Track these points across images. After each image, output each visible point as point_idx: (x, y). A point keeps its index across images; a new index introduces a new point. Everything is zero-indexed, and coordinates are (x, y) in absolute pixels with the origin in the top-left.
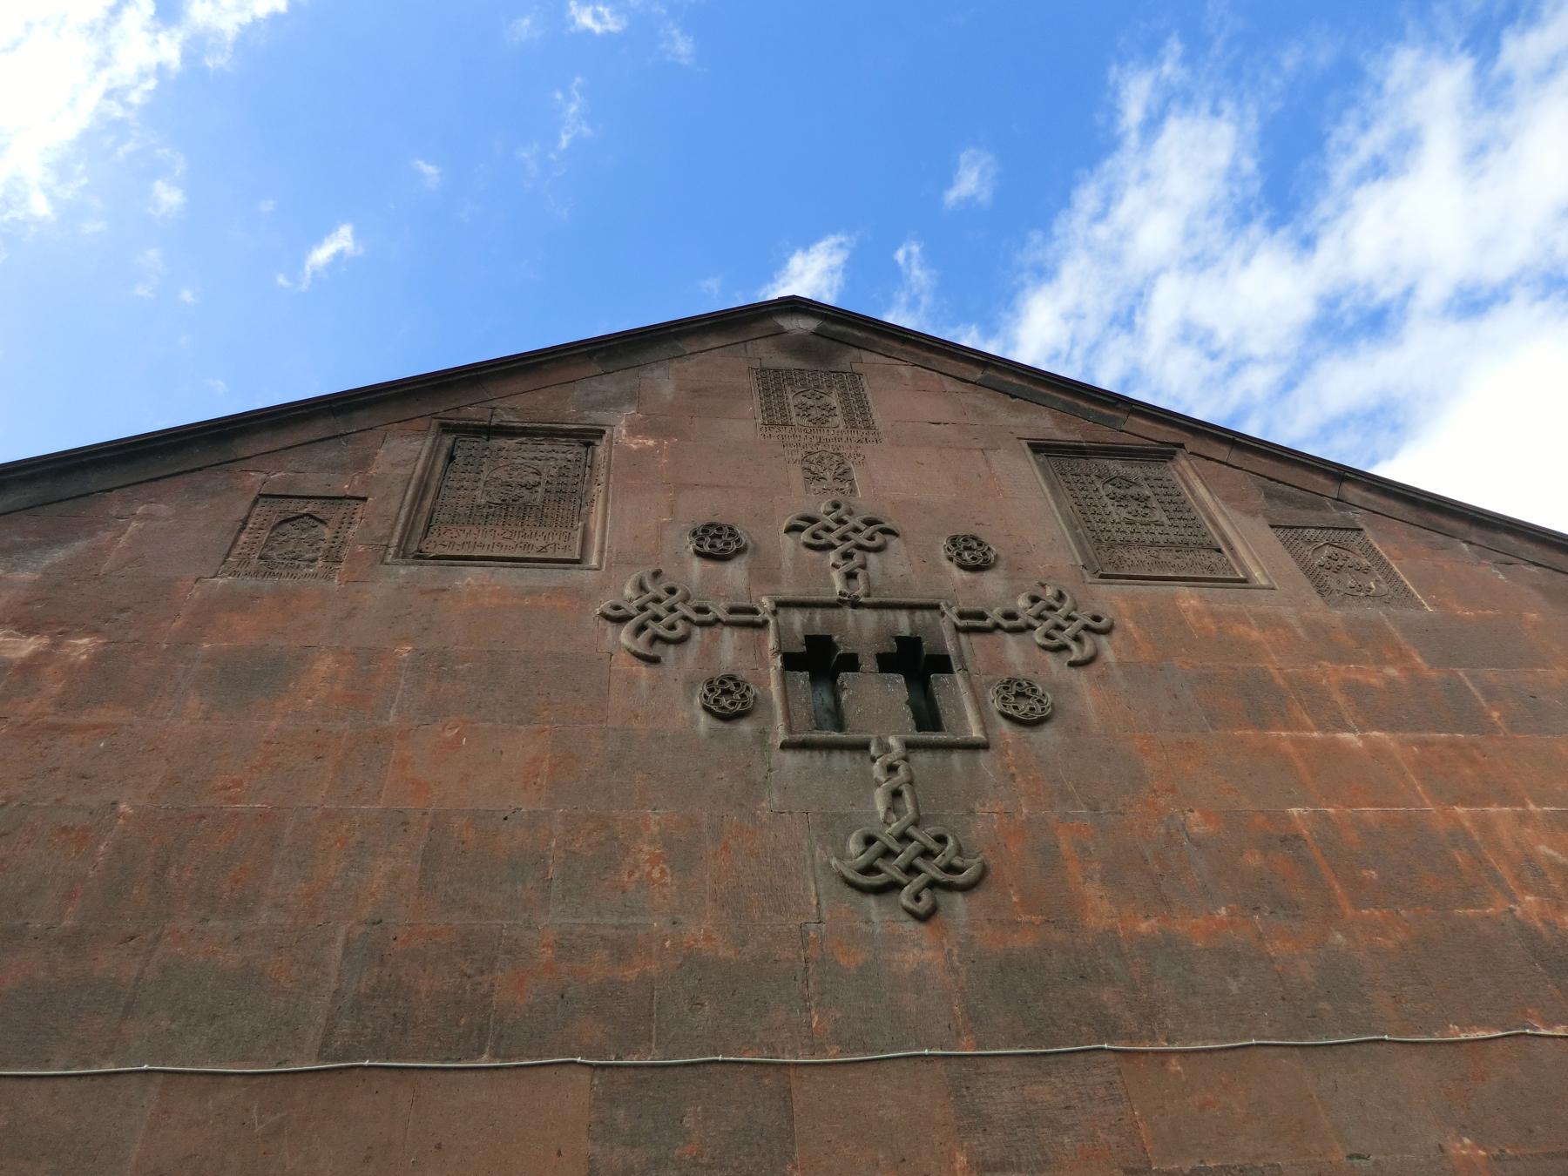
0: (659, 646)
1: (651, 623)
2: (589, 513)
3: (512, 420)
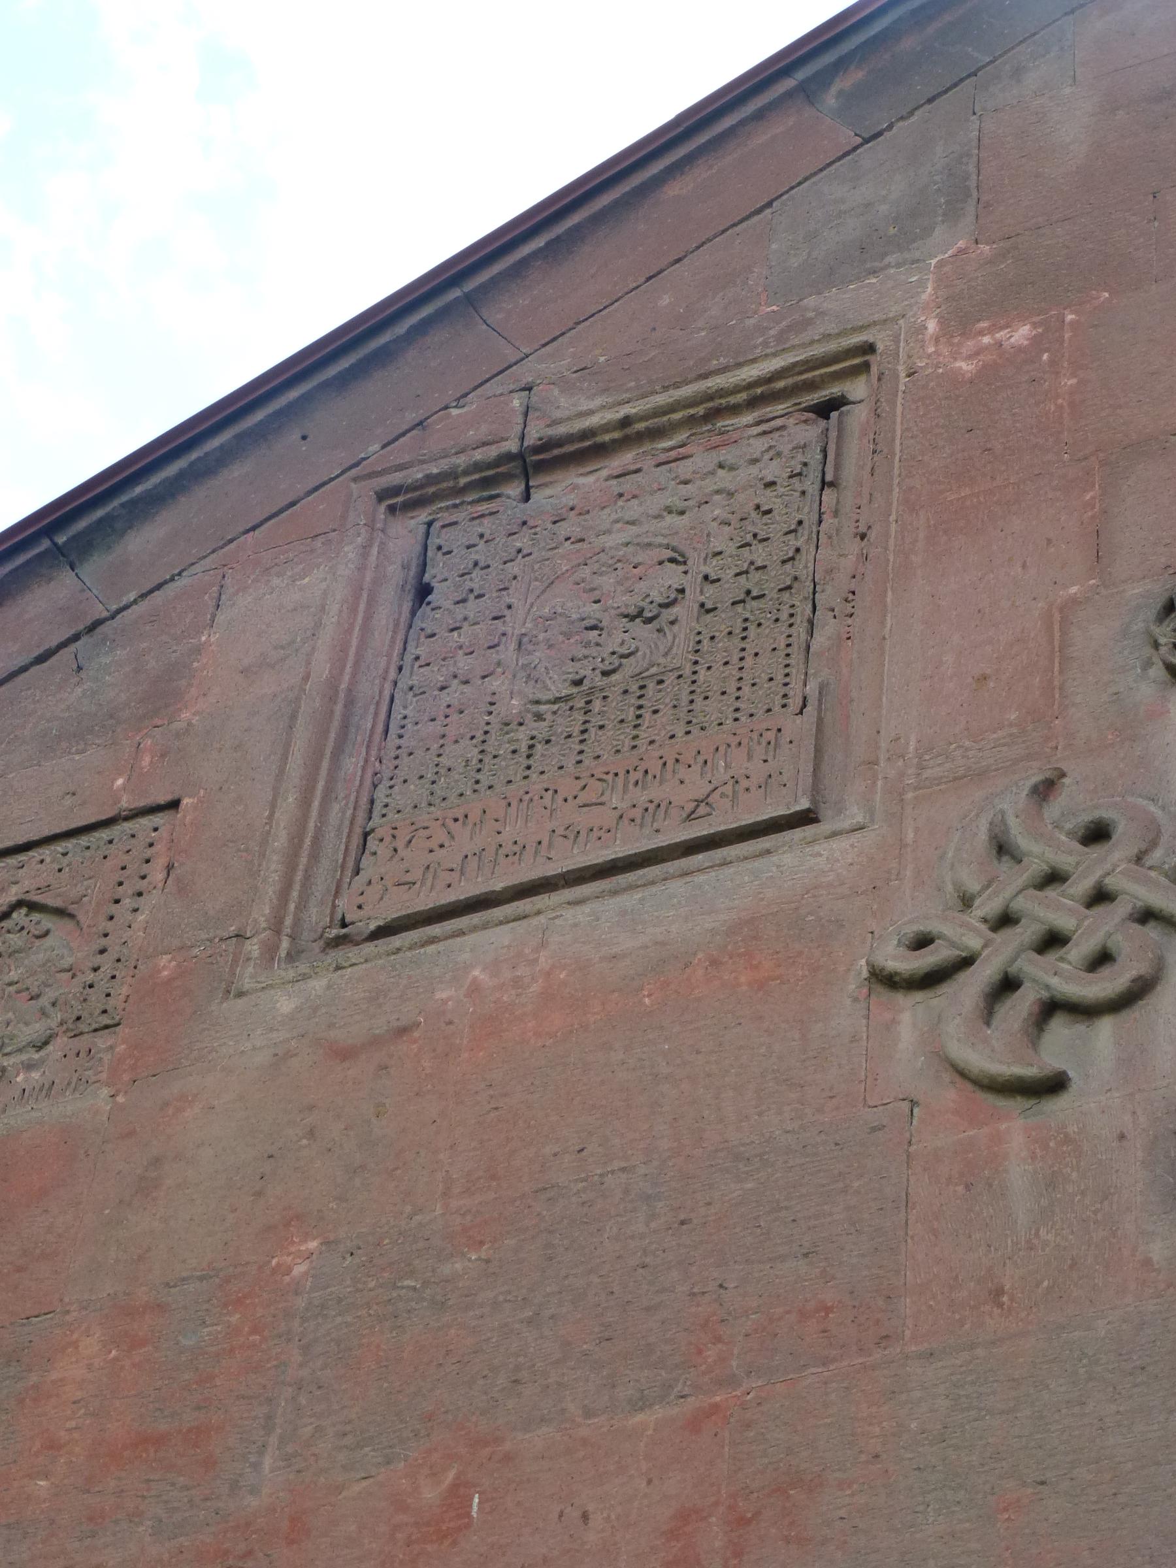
0: (1060, 1029)
3: (587, 409)
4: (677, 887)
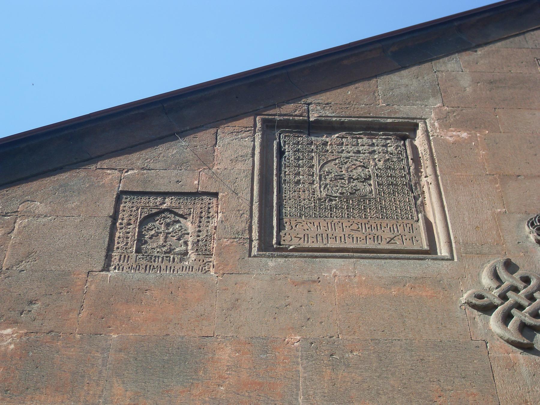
1: (514, 311)
2: (423, 204)
4: (395, 261)
